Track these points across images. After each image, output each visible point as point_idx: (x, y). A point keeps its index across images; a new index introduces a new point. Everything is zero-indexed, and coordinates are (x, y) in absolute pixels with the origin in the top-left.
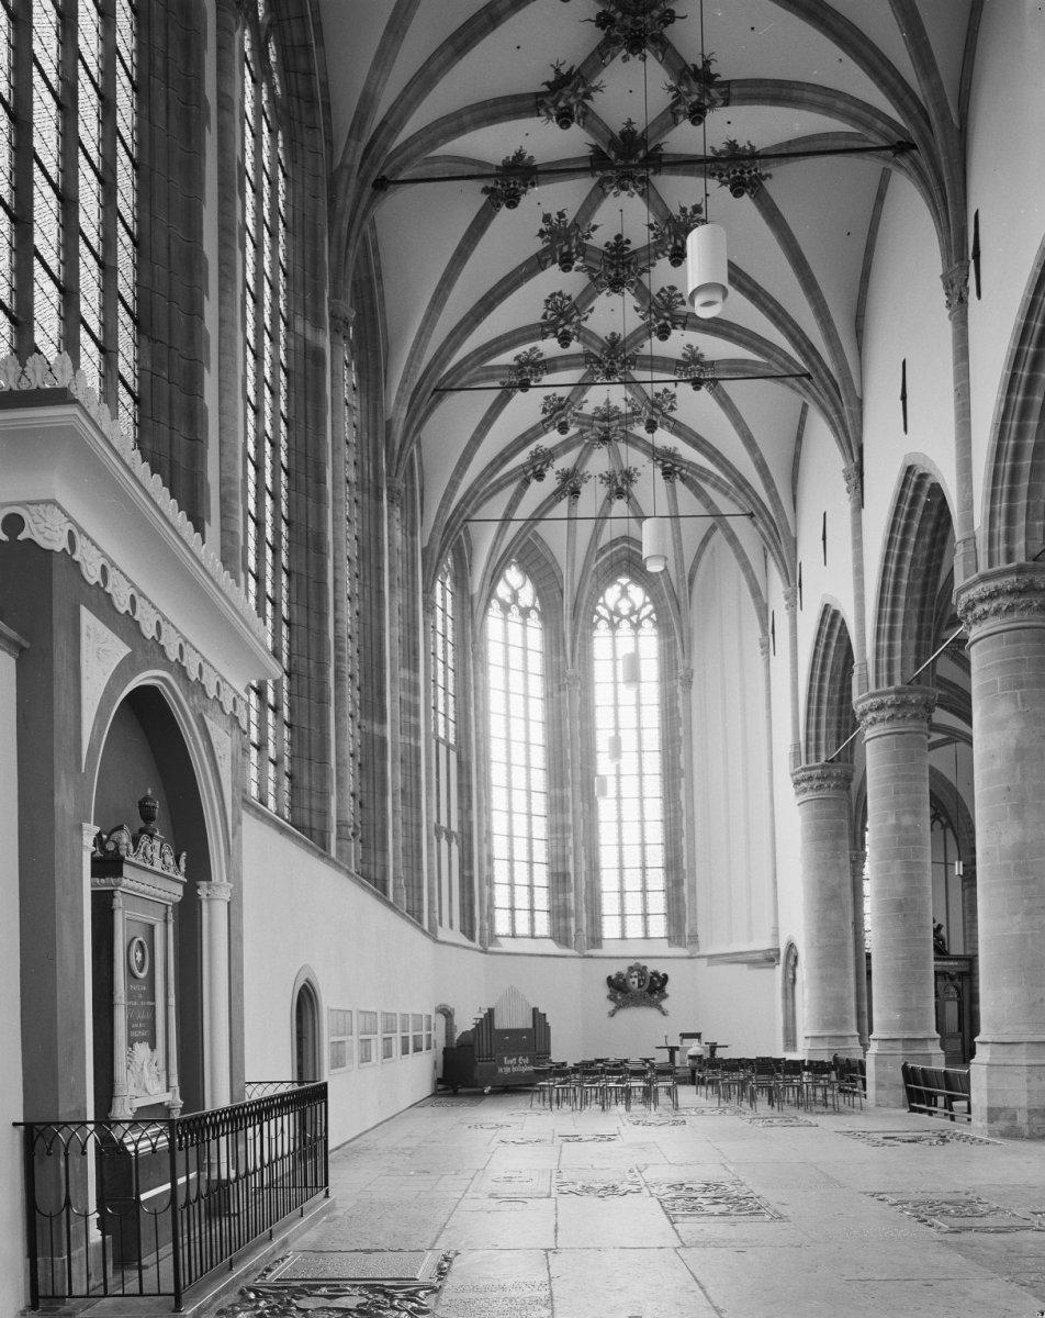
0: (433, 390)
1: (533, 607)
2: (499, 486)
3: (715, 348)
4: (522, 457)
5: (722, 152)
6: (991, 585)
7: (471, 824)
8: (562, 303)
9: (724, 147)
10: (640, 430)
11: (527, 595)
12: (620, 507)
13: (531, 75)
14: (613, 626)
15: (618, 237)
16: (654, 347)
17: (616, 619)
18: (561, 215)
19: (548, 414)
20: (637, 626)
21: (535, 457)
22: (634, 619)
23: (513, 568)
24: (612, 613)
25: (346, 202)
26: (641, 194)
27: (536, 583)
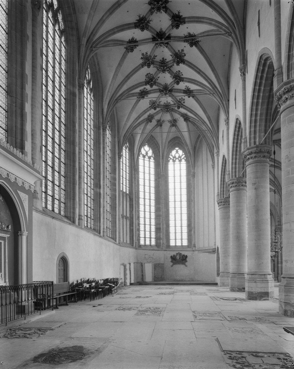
0: (115, 100)
1: (152, 156)
2: (139, 124)
3: (193, 87)
4: (146, 116)
5: (187, 35)
6: (250, 151)
7: (133, 215)
8: (150, 76)
9: (187, 34)
10: (176, 108)
11: (150, 153)
12: (174, 129)
13: (133, 19)
14: (174, 161)
15: (163, 58)
16: (176, 87)
17: (175, 159)
19: (151, 105)
20: (180, 161)
21: (149, 116)
22: (180, 159)
23: (146, 146)
24: (174, 157)
25: (82, 54)
26: (167, 47)
27: (152, 149)
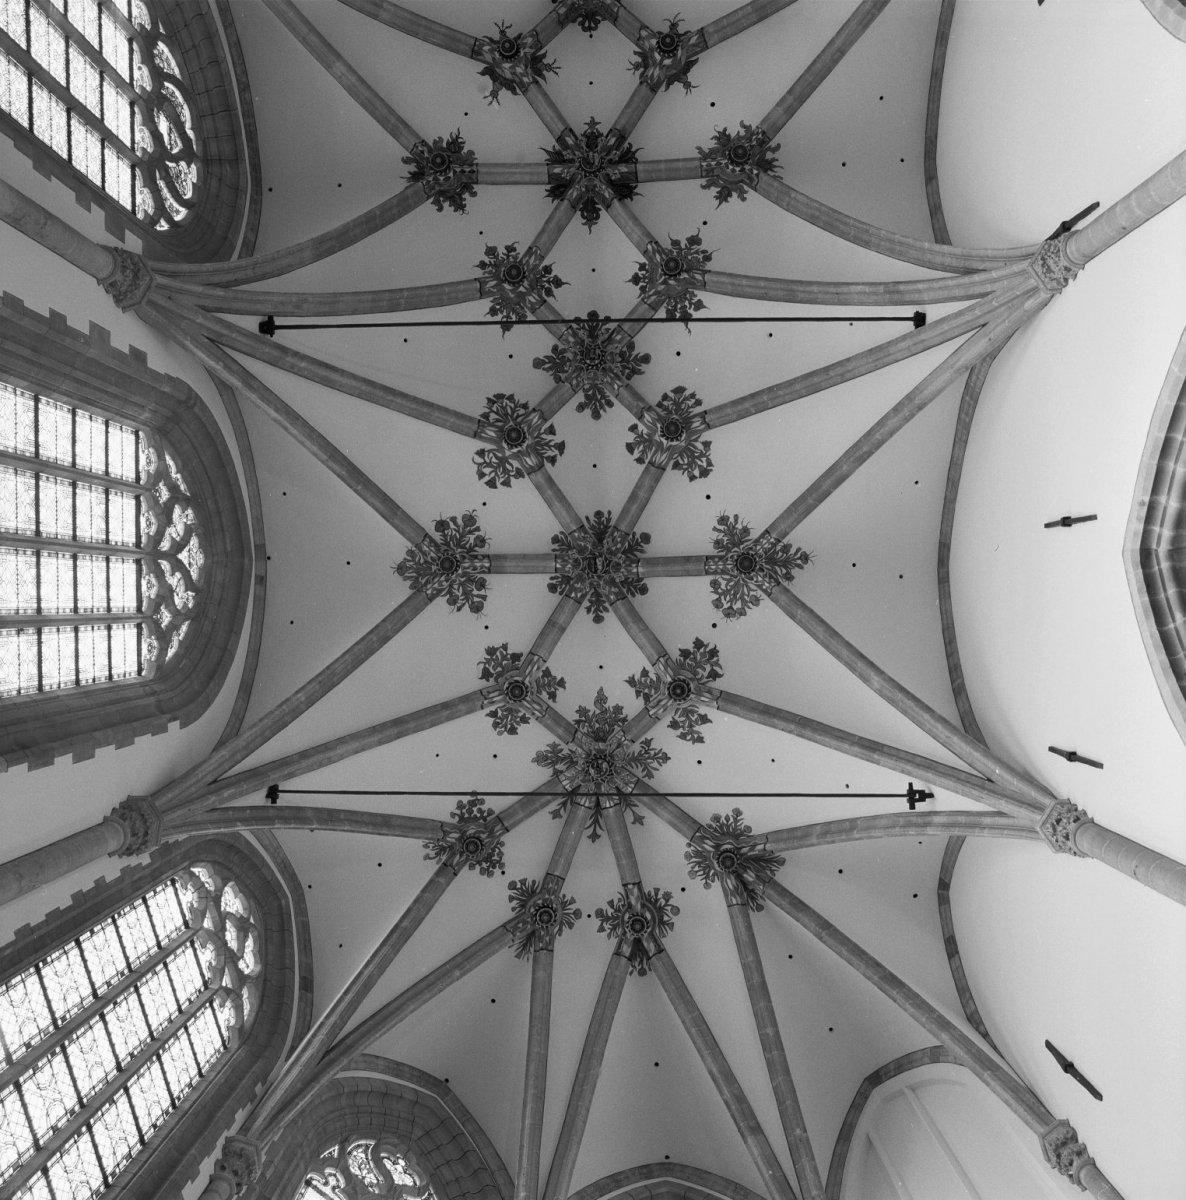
5: (712, 151)
8: (513, 411)
9: (713, 144)
18: (510, 249)
